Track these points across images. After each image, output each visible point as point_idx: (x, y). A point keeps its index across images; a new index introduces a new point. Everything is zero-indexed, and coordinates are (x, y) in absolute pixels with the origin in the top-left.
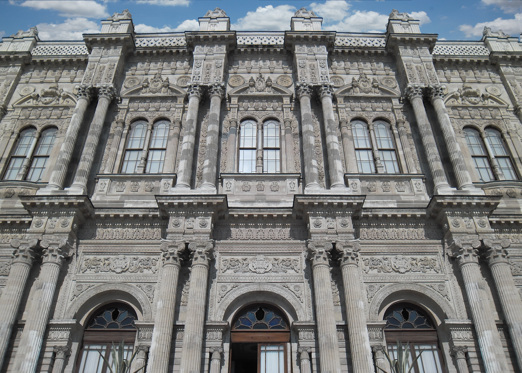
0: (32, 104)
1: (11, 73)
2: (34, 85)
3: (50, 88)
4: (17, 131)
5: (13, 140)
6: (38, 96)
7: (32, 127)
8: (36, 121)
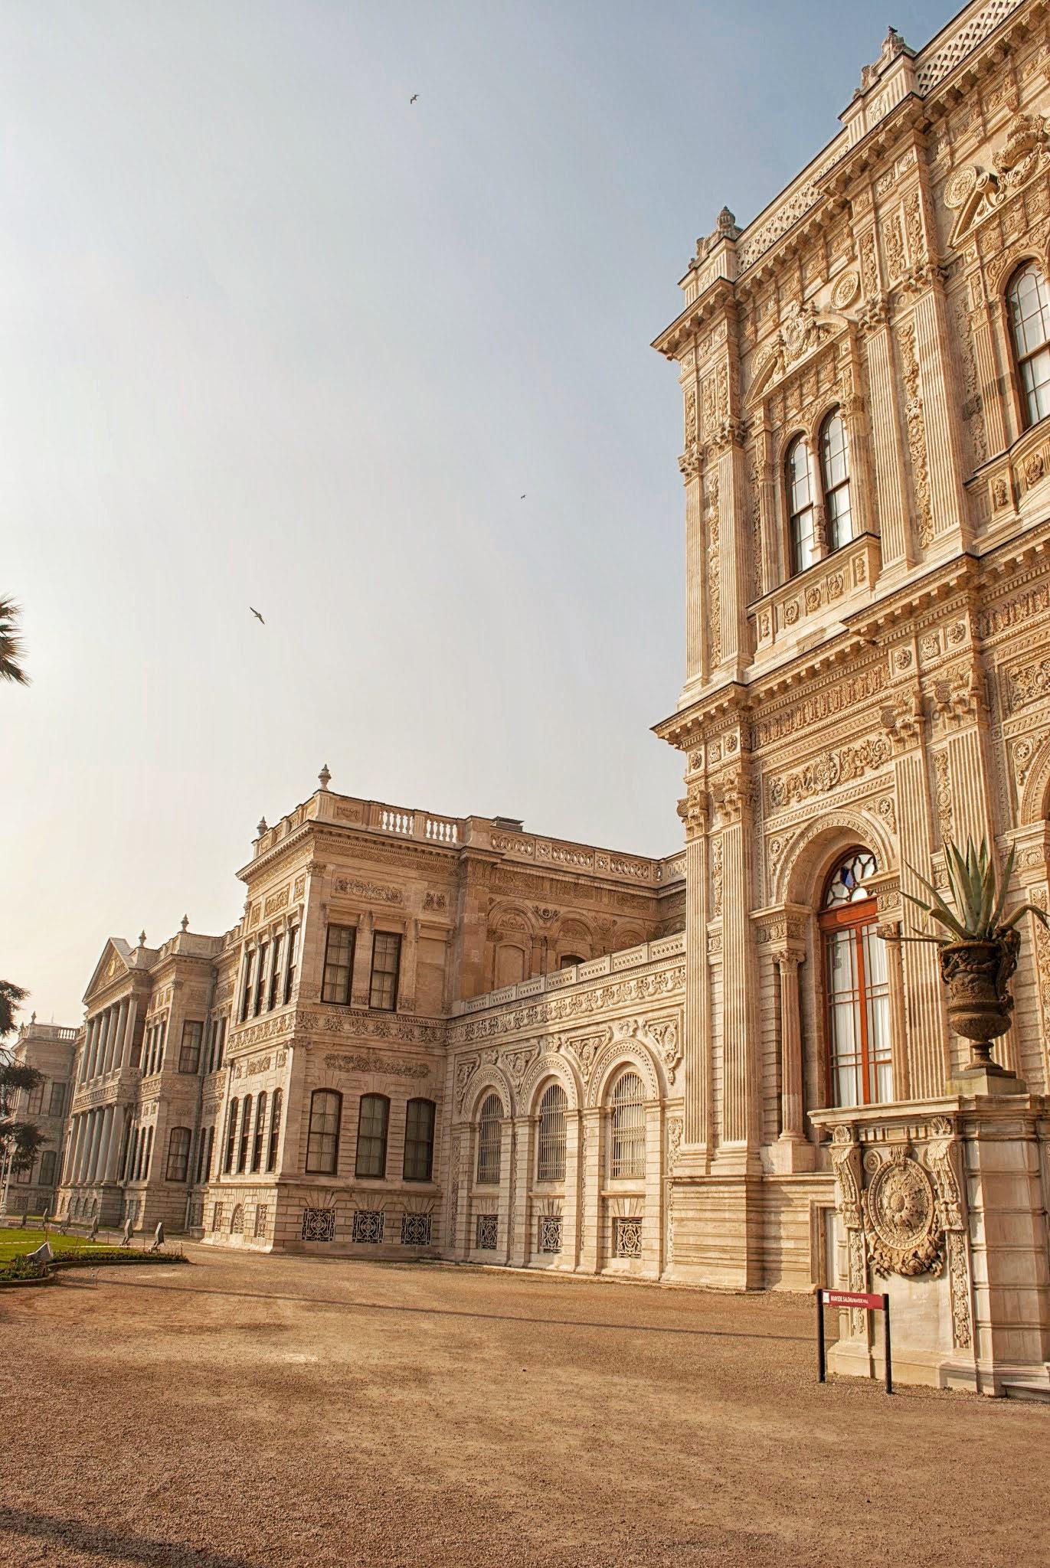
0: (991, 209)
1: (905, 177)
2: (969, 162)
3: (1010, 136)
4: (994, 297)
5: (1000, 324)
6: (993, 178)
7: (1023, 264)
8: (1023, 241)
